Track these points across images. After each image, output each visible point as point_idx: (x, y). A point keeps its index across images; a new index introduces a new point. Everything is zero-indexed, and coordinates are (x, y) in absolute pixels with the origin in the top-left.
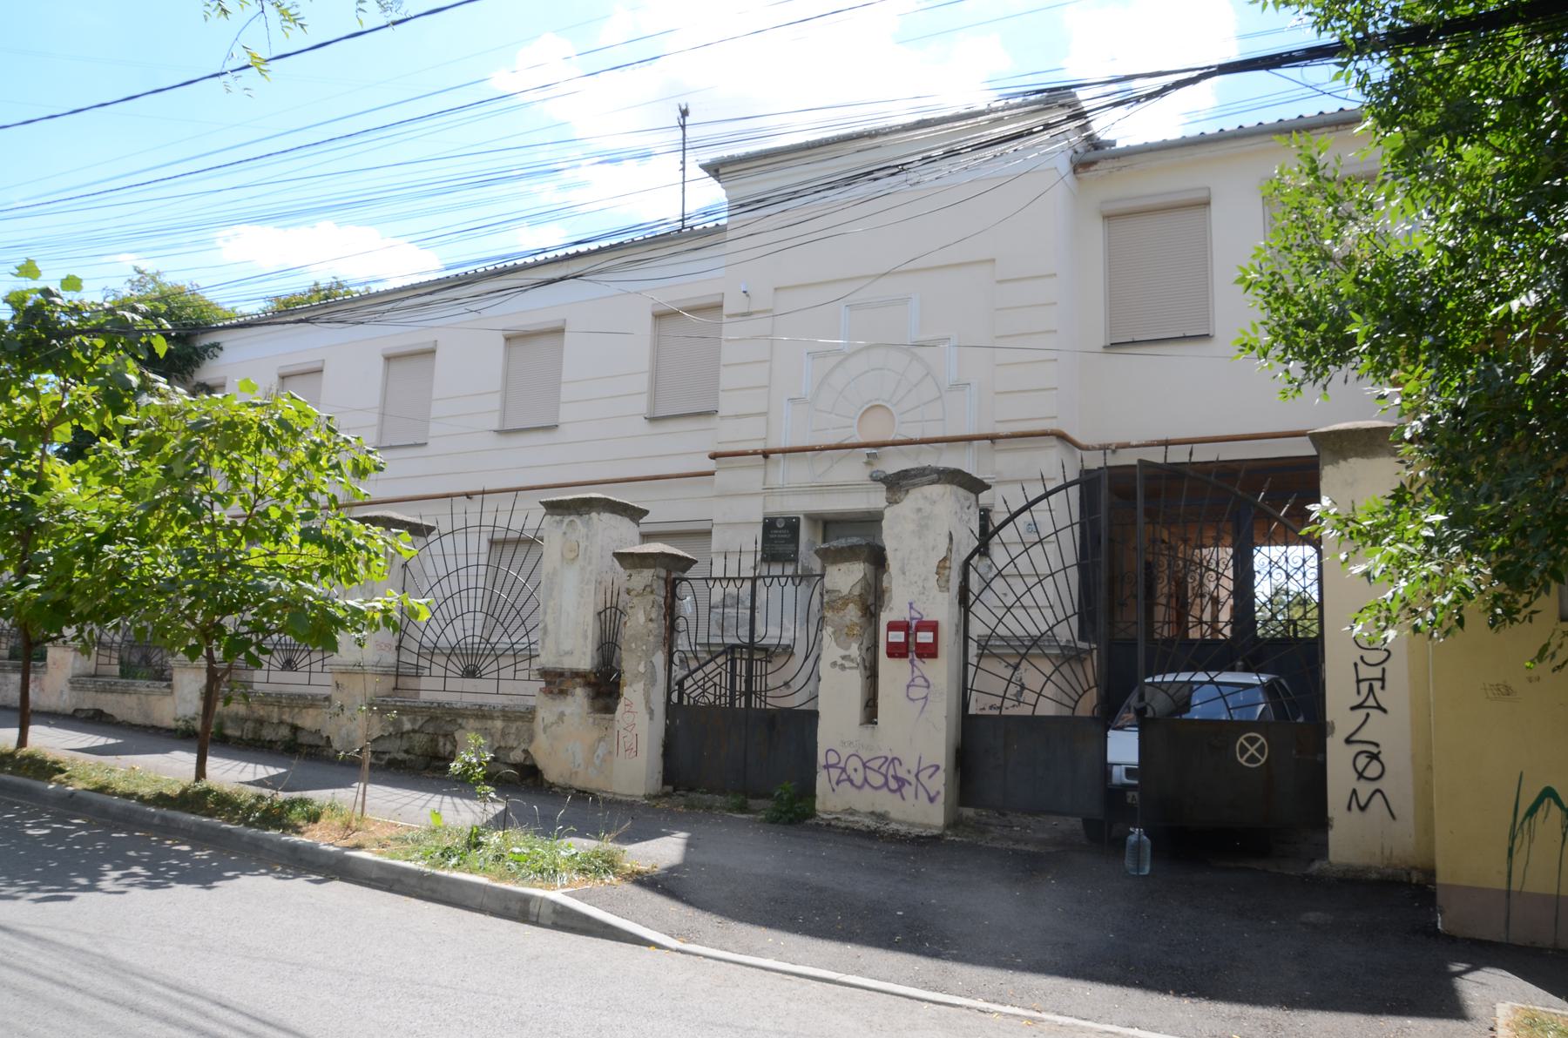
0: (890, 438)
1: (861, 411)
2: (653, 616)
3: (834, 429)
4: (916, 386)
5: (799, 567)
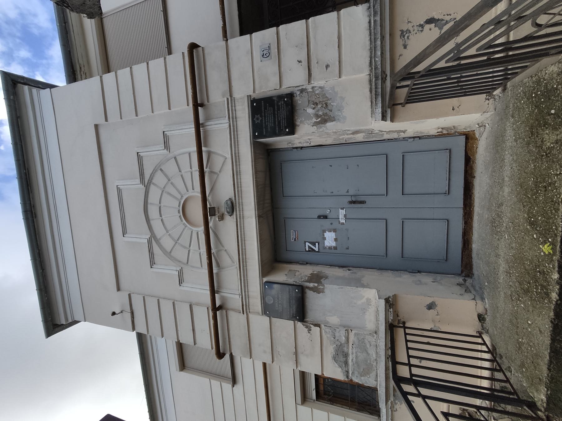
3: (199, 249)
4: (169, 180)
5: (311, 285)
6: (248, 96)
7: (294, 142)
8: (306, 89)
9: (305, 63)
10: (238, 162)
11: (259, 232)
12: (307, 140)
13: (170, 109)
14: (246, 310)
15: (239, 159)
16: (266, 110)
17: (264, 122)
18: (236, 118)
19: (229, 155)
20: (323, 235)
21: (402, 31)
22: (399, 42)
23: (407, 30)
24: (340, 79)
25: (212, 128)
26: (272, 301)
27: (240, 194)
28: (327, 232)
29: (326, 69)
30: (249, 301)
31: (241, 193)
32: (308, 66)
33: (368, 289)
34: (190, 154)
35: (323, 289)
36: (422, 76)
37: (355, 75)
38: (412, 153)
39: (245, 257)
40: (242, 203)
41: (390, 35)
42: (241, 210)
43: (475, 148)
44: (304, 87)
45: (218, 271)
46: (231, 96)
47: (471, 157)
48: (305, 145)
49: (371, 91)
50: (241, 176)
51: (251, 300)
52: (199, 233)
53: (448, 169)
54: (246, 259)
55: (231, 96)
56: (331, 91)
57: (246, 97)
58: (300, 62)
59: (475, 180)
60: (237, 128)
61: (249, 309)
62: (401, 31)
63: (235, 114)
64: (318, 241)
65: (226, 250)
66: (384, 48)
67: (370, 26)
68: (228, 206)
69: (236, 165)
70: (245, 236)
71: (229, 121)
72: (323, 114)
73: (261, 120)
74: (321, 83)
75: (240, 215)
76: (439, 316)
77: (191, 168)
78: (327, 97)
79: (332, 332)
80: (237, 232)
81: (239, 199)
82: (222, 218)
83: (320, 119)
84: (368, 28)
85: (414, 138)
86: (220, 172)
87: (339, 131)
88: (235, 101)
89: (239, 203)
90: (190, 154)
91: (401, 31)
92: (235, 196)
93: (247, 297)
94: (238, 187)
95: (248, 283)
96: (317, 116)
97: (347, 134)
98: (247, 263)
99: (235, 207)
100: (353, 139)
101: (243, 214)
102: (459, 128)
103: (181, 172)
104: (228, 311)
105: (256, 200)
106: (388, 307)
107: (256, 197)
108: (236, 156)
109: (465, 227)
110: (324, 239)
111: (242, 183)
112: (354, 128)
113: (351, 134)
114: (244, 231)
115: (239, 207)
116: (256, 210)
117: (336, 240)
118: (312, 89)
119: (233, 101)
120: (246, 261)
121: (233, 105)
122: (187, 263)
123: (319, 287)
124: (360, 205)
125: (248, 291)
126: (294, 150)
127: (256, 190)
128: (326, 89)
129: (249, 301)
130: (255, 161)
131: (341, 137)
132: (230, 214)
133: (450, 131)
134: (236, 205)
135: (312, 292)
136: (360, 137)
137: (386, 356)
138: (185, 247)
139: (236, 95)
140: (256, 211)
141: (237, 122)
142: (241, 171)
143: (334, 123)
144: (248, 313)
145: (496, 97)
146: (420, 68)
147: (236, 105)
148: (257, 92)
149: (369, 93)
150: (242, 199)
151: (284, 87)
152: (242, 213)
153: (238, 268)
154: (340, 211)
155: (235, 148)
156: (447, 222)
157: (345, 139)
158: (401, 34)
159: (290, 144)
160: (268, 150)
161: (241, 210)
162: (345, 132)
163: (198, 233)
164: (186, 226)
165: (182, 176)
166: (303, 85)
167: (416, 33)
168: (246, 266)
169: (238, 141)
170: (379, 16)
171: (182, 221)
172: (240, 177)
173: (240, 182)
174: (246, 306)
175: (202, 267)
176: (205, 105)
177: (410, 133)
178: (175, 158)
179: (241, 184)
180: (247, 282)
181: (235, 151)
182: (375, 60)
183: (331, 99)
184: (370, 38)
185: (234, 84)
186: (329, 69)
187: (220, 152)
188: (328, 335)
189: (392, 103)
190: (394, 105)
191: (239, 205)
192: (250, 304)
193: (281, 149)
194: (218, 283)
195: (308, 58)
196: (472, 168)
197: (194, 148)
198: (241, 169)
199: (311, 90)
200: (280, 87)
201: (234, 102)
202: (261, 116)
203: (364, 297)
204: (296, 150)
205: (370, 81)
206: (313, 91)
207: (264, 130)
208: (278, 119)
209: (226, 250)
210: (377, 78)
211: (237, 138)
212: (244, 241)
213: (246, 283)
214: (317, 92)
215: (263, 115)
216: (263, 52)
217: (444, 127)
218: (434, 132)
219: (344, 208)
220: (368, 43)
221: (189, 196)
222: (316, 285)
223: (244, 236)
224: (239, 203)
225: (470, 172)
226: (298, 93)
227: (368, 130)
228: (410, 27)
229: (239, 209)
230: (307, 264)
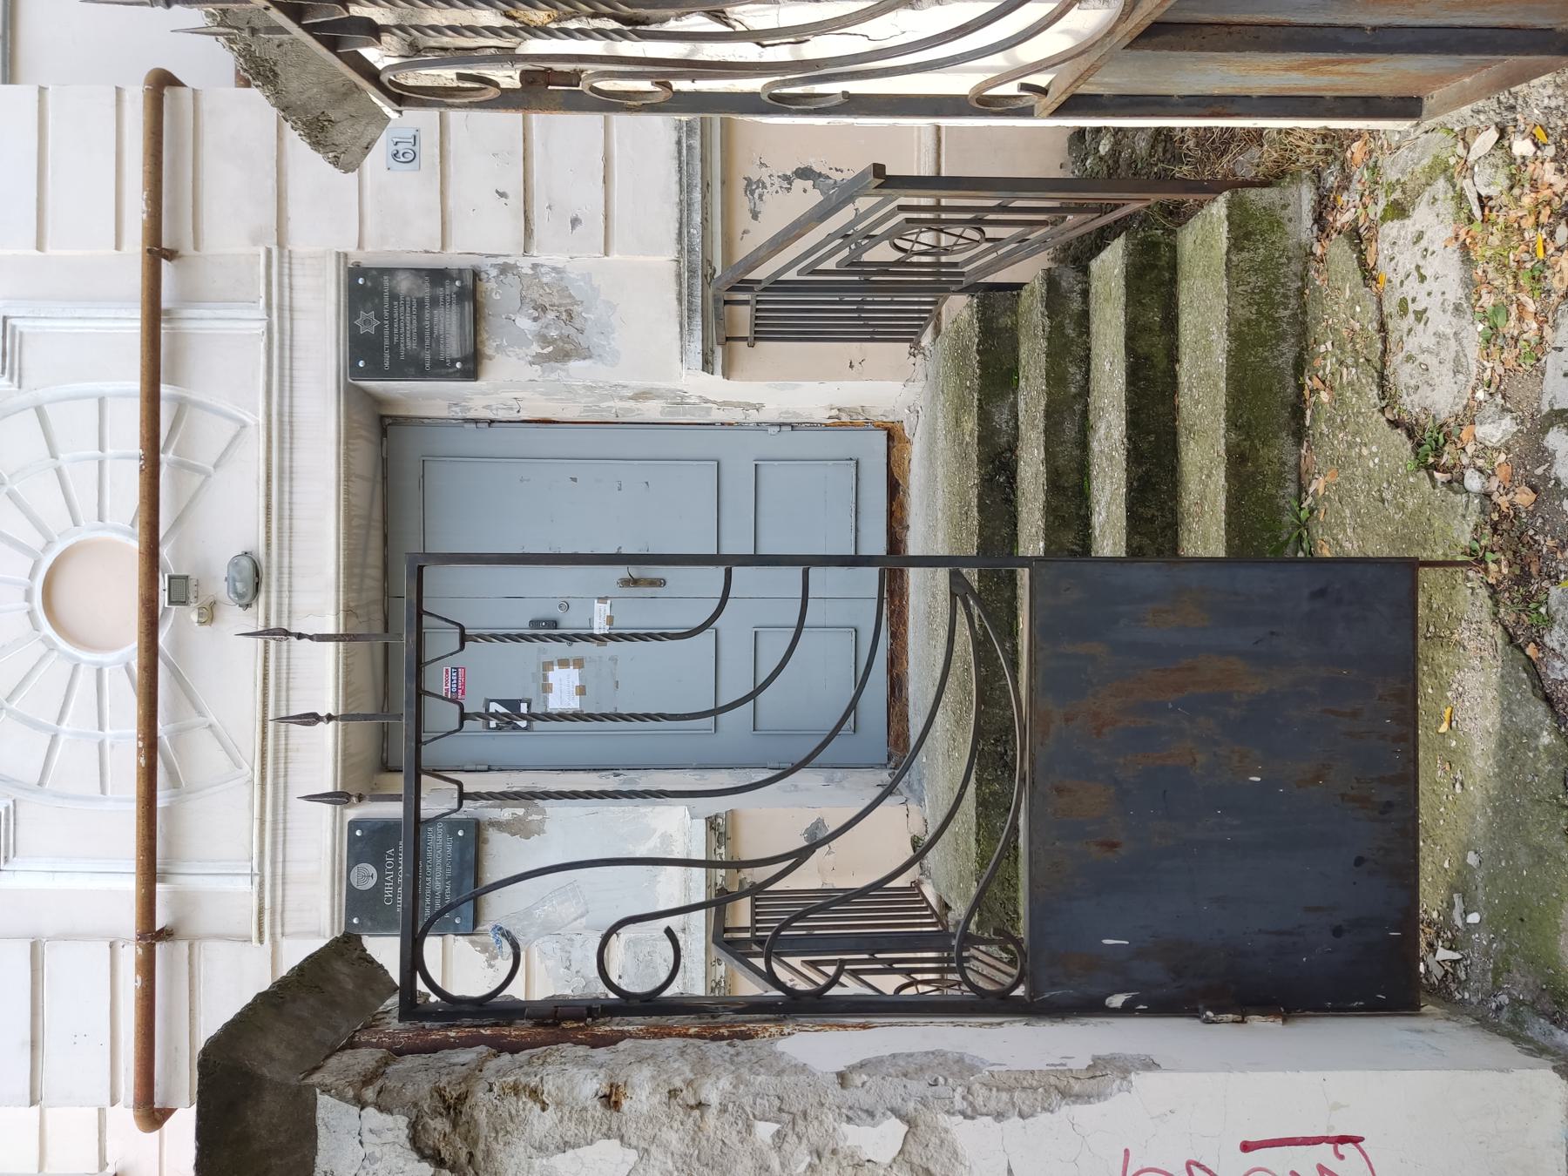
0: (133, 545)
1: (63, 645)
2: (589, 1085)
3: (101, 728)
6: (338, 254)
7: (470, 404)
8: (515, 267)
9: (516, 201)
10: (287, 440)
11: (346, 658)
12: (510, 403)
13: (40, 246)
14: (273, 926)
15: (291, 431)
16: (396, 303)
17: (386, 332)
18: (291, 310)
19: (257, 415)
20: (545, 678)
21: (748, 180)
22: (742, 204)
23: (759, 180)
24: (606, 258)
25: (201, 329)
26: (375, 878)
27: (286, 539)
28: (556, 668)
29: (573, 228)
30: (284, 896)
31: (290, 536)
32: (525, 212)
33: (667, 807)
34: (101, 401)
35: (542, 822)
36: (765, 289)
37: (643, 255)
38: (776, 463)
39: (286, 744)
40: (290, 567)
41: (723, 183)
42: (286, 588)
43: (907, 462)
44: (511, 261)
45: (171, 802)
46: (281, 244)
47: (901, 482)
48: (502, 415)
49: (680, 301)
50: (295, 483)
51: (292, 891)
52: (106, 671)
53: (854, 505)
54: (286, 750)
55: (281, 244)
56: (582, 284)
57: (334, 257)
58: (502, 195)
59: (908, 534)
60: (291, 340)
61: (283, 926)
62: (745, 178)
63: (291, 298)
64: (527, 696)
65: (210, 726)
66: (709, 209)
67: (680, 152)
68: (239, 572)
69: (281, 449)
70: (291, 675)
71: (269, 315)
72: (561, 337)
73: (379, 329)
74: (559, 260)
75: (280, 604)
76: (832, 855)
77: (101, 449)
78: (570, 296)
79: (562, 949)
80: (266, 660)
81: (280, 555)
82: (209, 614)
83: (551, 349)
84: (676, 154)
85: (781, 425)
86: (216, 466)
87: (601, 384)
88: (294, 261)
89: (280, 568)
90: (101, 401)
91: (745, 178)
92: (268, 545)
93: (279, 881)
94: (281, 518)
95: (288, 831)
96: (544, 340)
97: (621, 398)
98: (290, 766)
99: (264, 580)
100: (636, 412)
101: (290, 605)
102: (874, 412)
103: (57, 458)
104: (197, 944)
105: (341, 560)
106: (714, 843)
107: (344, 550)
108: (281, 422)
109: (891, 645)
110: (546, 688)
111: (294, 507)
112: (638, 383)
113: (630, 398)
114: (288, 658)
115: (279, 579)
116: (341, 589)
117: (581, 691)
118: (532, 269)
119: (287, 260)
120: (286, 757)
121: (286, 271)
122: (40, 784)
123: (530, 818)
124: (649, 591)
125: (284, 861)
126: (467, 425)
127: (344, 529)
128: (572, 276)
129: (284, 896)
130: (347, 443)
131: (604, 405)
132: (245, 601)
133: (855, 417)
134: (268, 574)
135: (506, 835)
136: (652, 410)
137: (709, 982)
138: (36, 725)
139: (300, 243)
140: (341, 593)
141: (295, 322)
142: (295, 470)
143: (587, 363)
144: (279, 936)
145: (927, 353)
146: (762, 273)
147: (294, 272)
148: (369, 249)
149: (676, 303)
150: (290, 556)
151: (453, 249)
152: (286, 601)
153: (257, 780)
154: (597, 605)
155: (281, 397)
156: (854, 633)
157: (614, 411)
158: (747, 185)
159: (458, 409)
160: (382, 418)
161: (286, 588)
162: (615, 390)
163: (100, 672)
164: (52, 647)
165: (59, 471)
166: (508, 256)
167: (777, 192)
168: (286, 775)
169: (291, 376)
170: (698, 137)
171: (36, 627)
172: (291, 487)
173: (290, 503)
174: (273, 913)
175: (103, 792)
176: (181, 257)
177: (770, 414)
178: (39, 410)
179: (291, 510)
180: (285, 829)
181: (281, 405)
182: (688, 232)
183: (582, 302)
184: (681, 179)
185: (294, 210)
186: (579, 228)
187: (227, 407)
188: (550, 963)
189: (724, 334)
190: (728, 339)
191: (280, 573)
192: (289, 905)
193: (426, 421)
194: (169, 844)
195: (525, 189)
196: (902, 507)
197: (133, 384)
198: (295, 464)
199: (530, 272)
200: (443, 247)
201: (290, 263)
202: (379, 316)
203: (655, 831)
204: (474, 426)
205: (679, 276)
206: (535, 276)
207: (387, 356)
208: (391, 339)
209: (210, 726)
210: (692, 272)
211: (291, 369)
212: (288, 689)
213: (280, 832)
214: (545, 280)
215: (386, 314)
216: (395, 148)
217: (842, 406)
218: (821, 416)
219: (607, 598)
220: (675, 188)
221: (77, 543)
222: (521, 814)
223: (288, 673)
224: (280, 568)
225: (897, 514)
226: (494, 272)
227: (673, 391)
228: (763, 174)
229: (280, 586)
230: (489, 770)
